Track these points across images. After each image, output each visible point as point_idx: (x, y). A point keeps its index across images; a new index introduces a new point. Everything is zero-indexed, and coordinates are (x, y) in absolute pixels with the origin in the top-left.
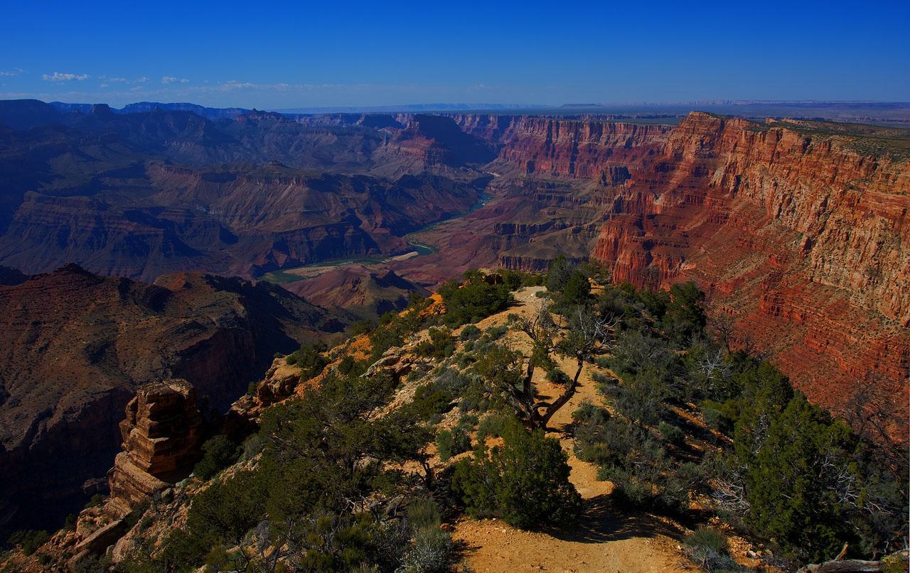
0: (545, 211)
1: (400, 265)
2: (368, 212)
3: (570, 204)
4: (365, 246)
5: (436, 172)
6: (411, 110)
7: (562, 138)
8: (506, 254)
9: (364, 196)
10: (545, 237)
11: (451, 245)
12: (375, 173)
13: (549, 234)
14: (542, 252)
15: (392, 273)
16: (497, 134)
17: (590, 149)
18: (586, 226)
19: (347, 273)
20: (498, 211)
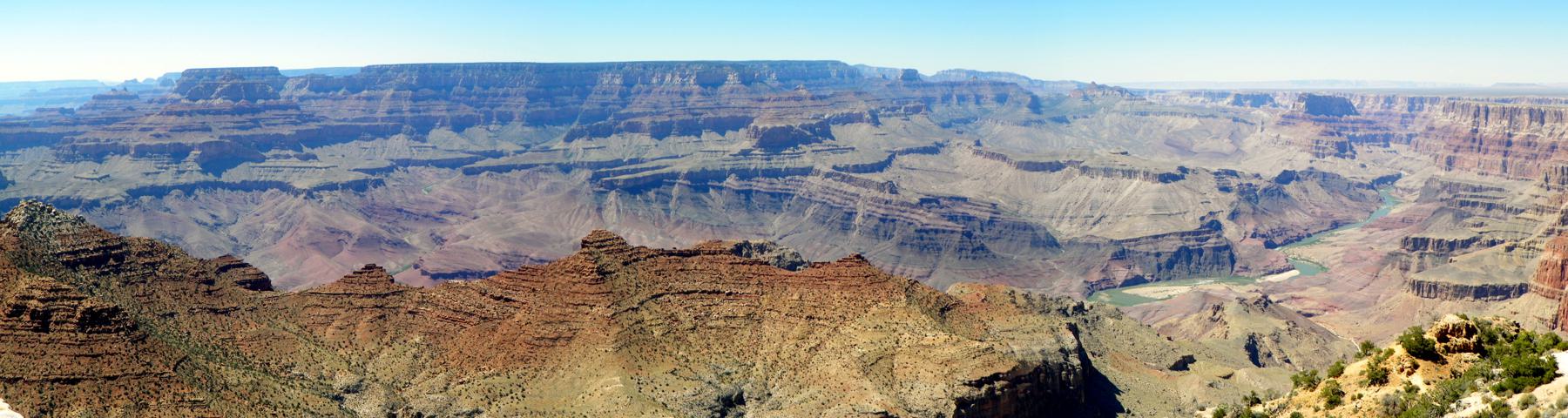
0: (1470, 221)
1: (1276, 288)
2: (1233, 216)
3: (1502, 213)
4: (1224, 259)
5: (1325, 168)
6: (1296, 87)
7: (1491, 128)
8: (1419, 277)
9: (1232, 197)
10: (1468, 257)
11: (1345, 263)
12: (1246, 167)
13: (1475, 252)
14: (1465, 275)
15: (1265, 297)
16: (1404, 122)
17: (1529, 143)
18: (1523, 243)
19: (1206, 296)
20: (1405, 221)
